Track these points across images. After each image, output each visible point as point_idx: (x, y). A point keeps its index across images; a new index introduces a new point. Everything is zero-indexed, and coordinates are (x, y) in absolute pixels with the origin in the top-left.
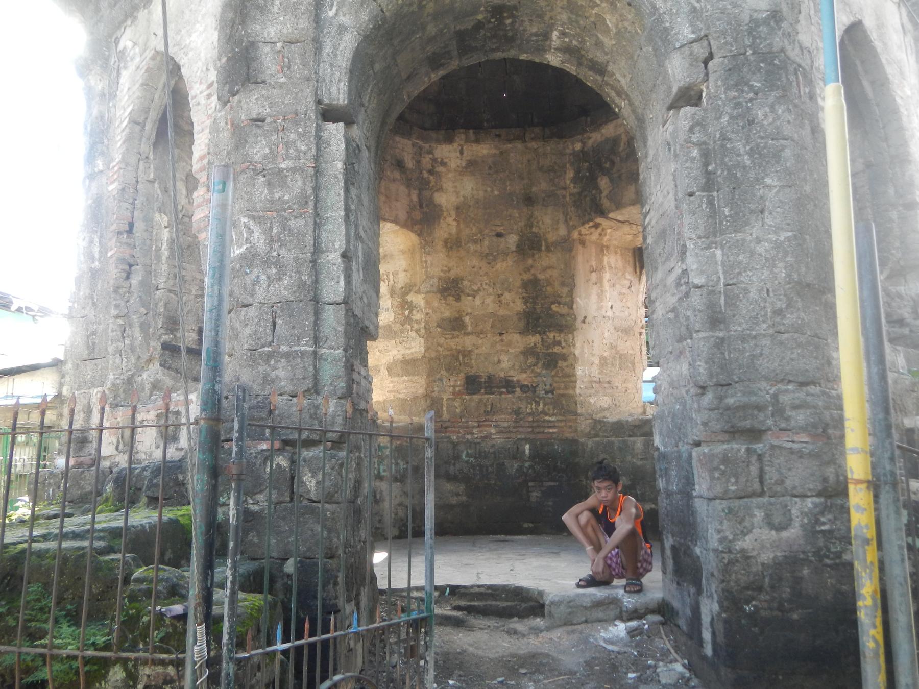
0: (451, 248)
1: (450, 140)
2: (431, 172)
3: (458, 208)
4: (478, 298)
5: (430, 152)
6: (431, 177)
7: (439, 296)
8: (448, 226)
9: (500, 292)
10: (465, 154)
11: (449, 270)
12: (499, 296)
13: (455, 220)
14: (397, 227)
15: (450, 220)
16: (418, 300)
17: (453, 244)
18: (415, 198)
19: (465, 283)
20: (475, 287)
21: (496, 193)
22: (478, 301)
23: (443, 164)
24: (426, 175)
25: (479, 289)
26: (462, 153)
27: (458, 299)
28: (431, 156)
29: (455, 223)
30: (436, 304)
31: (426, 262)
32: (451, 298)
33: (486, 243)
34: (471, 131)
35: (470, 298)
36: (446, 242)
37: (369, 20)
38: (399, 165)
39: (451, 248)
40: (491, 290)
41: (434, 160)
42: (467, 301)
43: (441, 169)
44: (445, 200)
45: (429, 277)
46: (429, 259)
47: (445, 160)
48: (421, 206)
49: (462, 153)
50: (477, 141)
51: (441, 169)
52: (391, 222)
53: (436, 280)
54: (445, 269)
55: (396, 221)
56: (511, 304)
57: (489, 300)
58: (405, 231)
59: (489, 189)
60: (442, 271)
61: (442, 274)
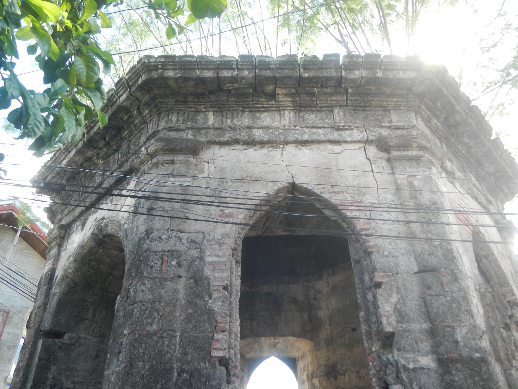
0: (329, 344)
1: (320, 278)
2: (315, 299)
3: (330, 317)
4: (346, 376)
5: (313, 288)
6: (315, 302)
7: (325, 378)
8: (326, 331)
9: (358, 370)
10: (330, 283)
11: (329, 359)
12: (358, 372)
13: (329, 325)
14: (295, 338)
15: (327, 326)
16: (316, 381)
17: (330, 342)
18: (306, 317)
19: (339, 366)
20: (344, 368)
21: (348, 303)
22: (347, 378)
23: (320, 292)
24: (312, 301)
25: (347, 370)
26: (328, 283)
27: (336, 379)
28: (314, 290)
29: (329, 328)
30: (324, 384)
31: (317, 356)
32: (332, 378)
33: (347, 336)
34: (330, 269)
35: (342, 376)
36: (326, 340)
37: (65, 287)
38: (294, 301)
39: (329, 344)
40: (353, 369)
41: (316, 291)
42: (341, 378)
43: (319, 296)
44: (323, 314)
45: (320, 366)
46: (318, 353)
47: (321, 290)
48: (311, 321)
49: (328, 283)
50: (334, 274)
51: (319, 296)
52: (290, 336)
53: (323, 367)
54: (327, 358)
55: (293, 335)
56: (366, 377)
57: (352, 377)
58: (300, 339)
59: (344, 301)
60: (326, 360)
61: (326, 363)
